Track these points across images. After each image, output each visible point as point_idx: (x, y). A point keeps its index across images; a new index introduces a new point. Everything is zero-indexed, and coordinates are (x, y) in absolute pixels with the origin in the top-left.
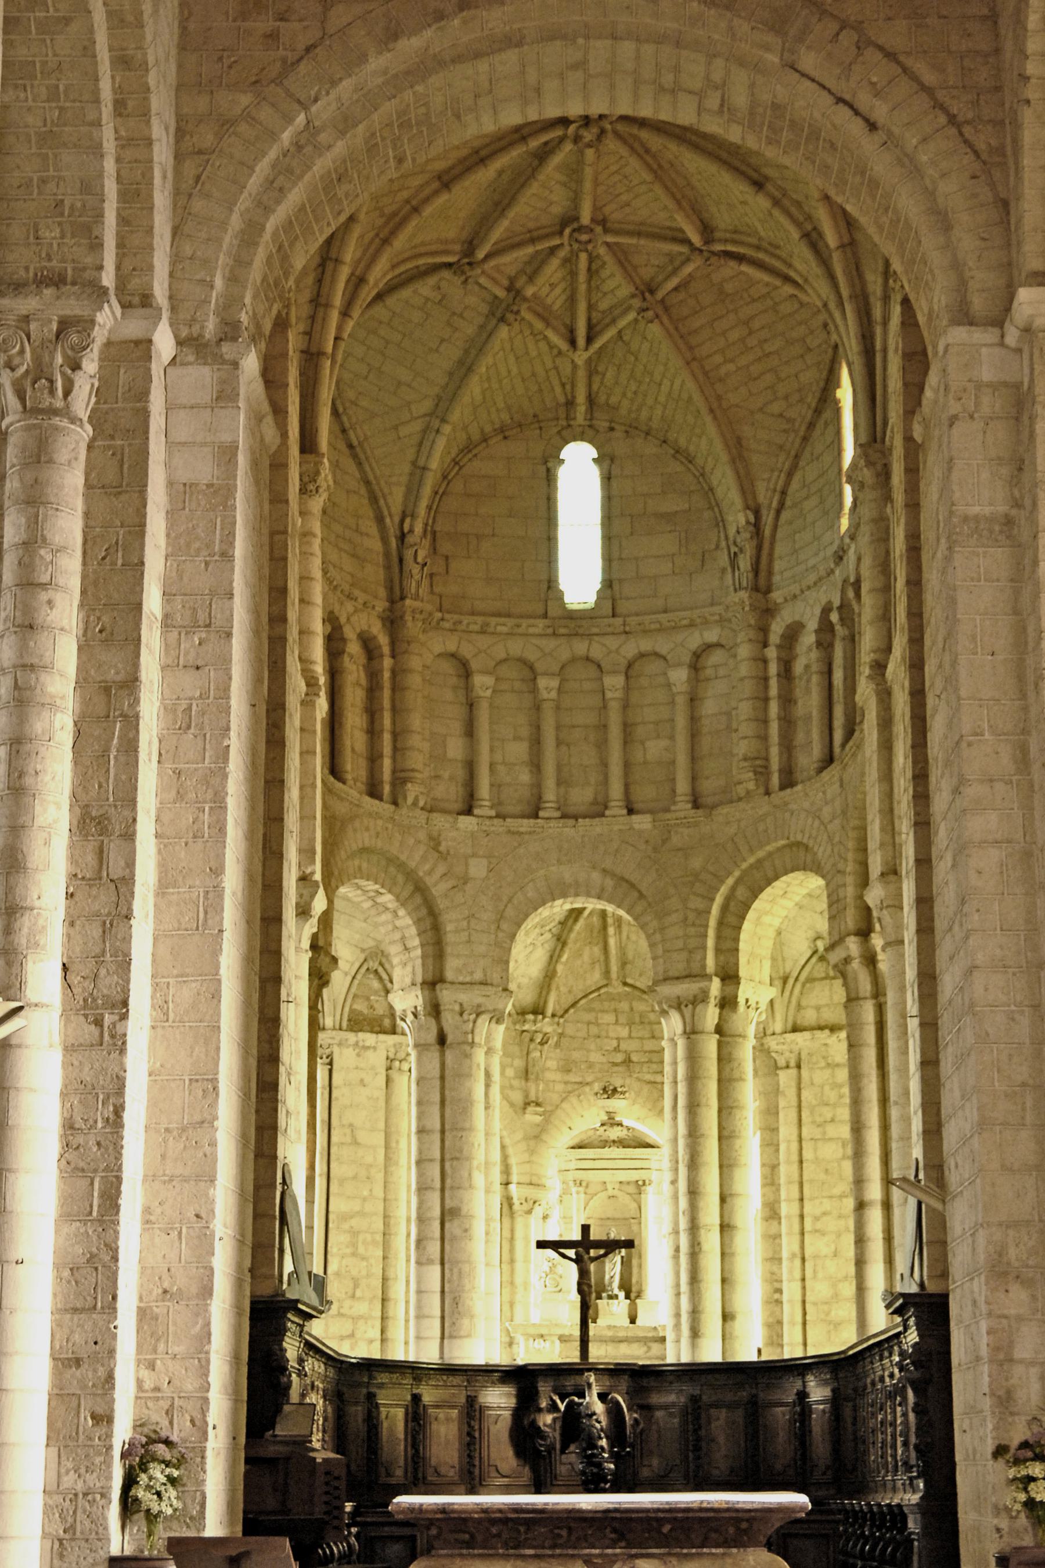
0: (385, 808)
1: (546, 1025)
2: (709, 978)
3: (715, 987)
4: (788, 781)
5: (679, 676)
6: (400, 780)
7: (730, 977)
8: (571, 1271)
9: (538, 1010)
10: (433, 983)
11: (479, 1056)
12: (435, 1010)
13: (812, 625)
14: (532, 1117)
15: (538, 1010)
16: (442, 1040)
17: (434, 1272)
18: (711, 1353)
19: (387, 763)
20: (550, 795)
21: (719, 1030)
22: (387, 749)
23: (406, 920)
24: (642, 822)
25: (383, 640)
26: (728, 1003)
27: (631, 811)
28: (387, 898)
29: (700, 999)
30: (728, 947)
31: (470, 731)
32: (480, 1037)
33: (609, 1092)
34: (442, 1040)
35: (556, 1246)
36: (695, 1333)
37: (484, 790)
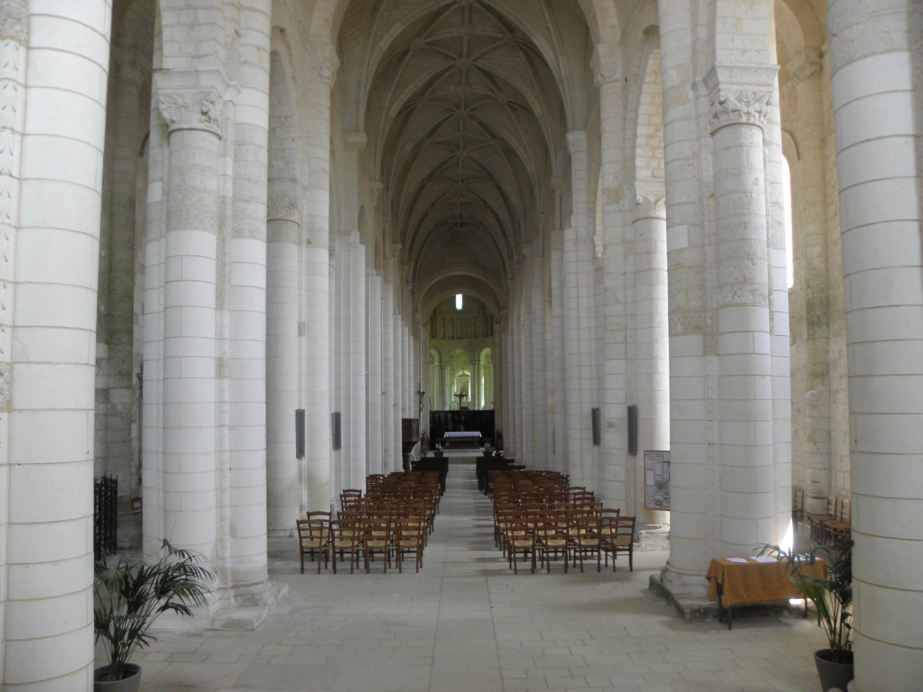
0: (433, 339)
1: (454, 359)
2: (475, 361)
3: (477, 362)
4: (487, 336)
5: (472, 320)
6: (436, 336)
7: (479, 361)
8: (458, 399)
9: (453, 357)
10: (440, 362)
11: (447, 371)
12: (440, 365)
13: (490, 316)
14: (453, 372)
15: (453, 357)
16: (441, 369)
17: (441, 399)
18: (477, 409)
19: (434, 333)
20: (455, 336)
21: (478, 367)
22: (434, 331)
23: (436, 353)
24: (467, 340)
25: (433, 317)
26: (479, 364)
27: (466, 338)
28: (434, 351)
29: (475, 364)
30: (479, 357)
31: (445, 328)
32: (447, 369)
33: (463, 369)
34: (441, 369)
35: (457, 395)
36: (474, 406)
37: (447, 336)
